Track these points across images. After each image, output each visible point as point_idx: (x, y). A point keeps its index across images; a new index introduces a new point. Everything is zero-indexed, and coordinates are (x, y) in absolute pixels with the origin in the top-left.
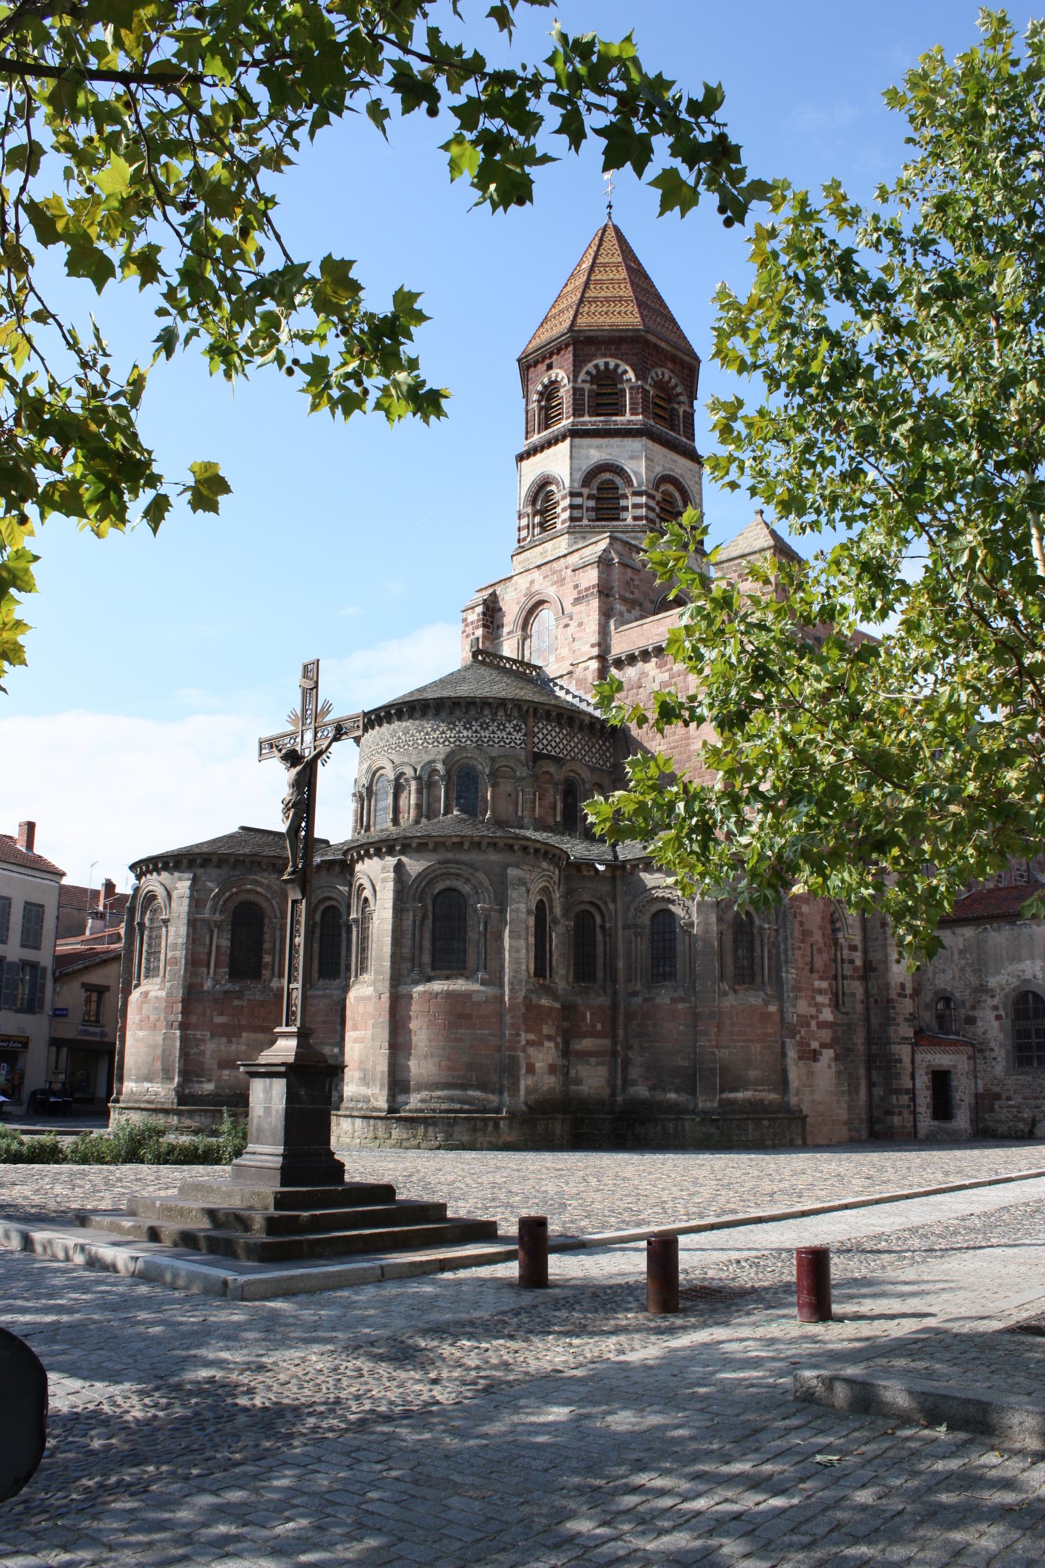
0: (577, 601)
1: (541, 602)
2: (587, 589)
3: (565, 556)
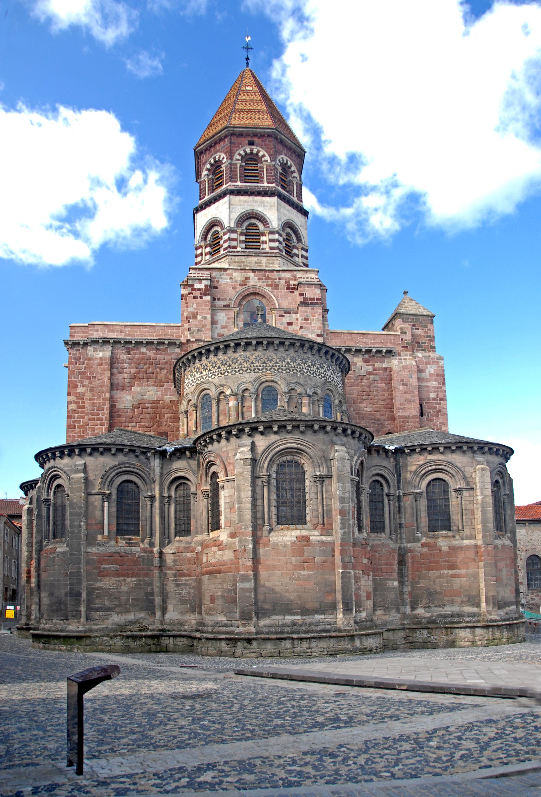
0: (302, 304)
1: (255, 294)
2: (311, 299)
3: (278, 271)
